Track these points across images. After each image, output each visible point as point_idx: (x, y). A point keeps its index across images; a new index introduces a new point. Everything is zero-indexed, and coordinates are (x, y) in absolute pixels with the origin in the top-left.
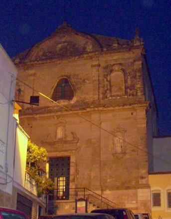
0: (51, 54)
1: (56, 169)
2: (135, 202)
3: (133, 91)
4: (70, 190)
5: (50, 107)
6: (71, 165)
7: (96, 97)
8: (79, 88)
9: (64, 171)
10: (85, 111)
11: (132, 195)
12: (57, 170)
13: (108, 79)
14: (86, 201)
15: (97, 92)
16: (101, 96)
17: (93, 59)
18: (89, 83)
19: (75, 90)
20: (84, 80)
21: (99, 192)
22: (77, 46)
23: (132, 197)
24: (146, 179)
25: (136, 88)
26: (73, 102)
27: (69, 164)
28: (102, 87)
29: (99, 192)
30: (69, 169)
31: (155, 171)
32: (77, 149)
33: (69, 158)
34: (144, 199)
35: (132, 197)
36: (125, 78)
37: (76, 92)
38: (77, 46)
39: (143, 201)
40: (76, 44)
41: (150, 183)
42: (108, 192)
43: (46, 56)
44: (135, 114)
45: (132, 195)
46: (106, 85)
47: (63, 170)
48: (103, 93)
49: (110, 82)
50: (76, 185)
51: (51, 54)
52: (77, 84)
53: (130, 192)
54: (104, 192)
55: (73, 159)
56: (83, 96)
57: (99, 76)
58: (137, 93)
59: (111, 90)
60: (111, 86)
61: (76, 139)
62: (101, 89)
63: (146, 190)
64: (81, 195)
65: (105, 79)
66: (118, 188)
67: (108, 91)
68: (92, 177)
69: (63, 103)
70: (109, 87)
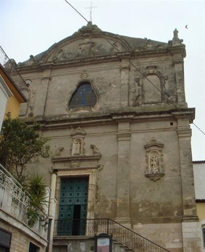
0: (71, 56)
1: (69, 194)
2: (178, 240)
3: (171, 97)
4: (88, 221)
5: (66, 115)
6: (89, 188)
7: (125, 103)
8: (104, 93)
9: (79, 196)
10: (110, 119)
11: (173, 231)
12: (71, 195)
13: (140, 83)
14: (110, 237)
15: (126, 97)
16: (132, 103)
17: (122, 60)
18: (116, 88)
19: (99, 95)
20: (110, 84)
21: (128, 225)
22: (103, 47)
23: (174, 233)
24: (194, 208)
25: (175, 94)
26: (94, 110)
27: (87, 188)
28: (133, 93)
29: (128, 225)
30: (87, 194)
31: (182, 69)
32: (99, 167)
33: (86, 178)
34: (191, 236)
35: (174, 233)
36: (161, 82)
37: (99, 98)
38: (103, 47)
39: (189, 238)
40: (102, 45)
41: (198, 215)
42: (139, 226)
43: (65, 57)
44: (175, 124)
45: (173, 231)
46: (137, 90)
47: (78, 194)
48: (133, 100)
49: (142, 86)
50: (96, 215)
51: (71, 56)
52: (100, 89)
53: (172, 226)
54: (135, 226)
55: (92, 181)
56: (108, 103)
57: (129, 80)
58: (177, 99)
59: (143, 96)
60: (143, 91)
61: (97, 158)
62: (131, 94)
63: (193, 224)
64: (102, 229)
65: (137, 84)
66: (154, 221)
67: (140, 97)
68: (118, 205)
69: (83, 111)
70: (141, 92)
